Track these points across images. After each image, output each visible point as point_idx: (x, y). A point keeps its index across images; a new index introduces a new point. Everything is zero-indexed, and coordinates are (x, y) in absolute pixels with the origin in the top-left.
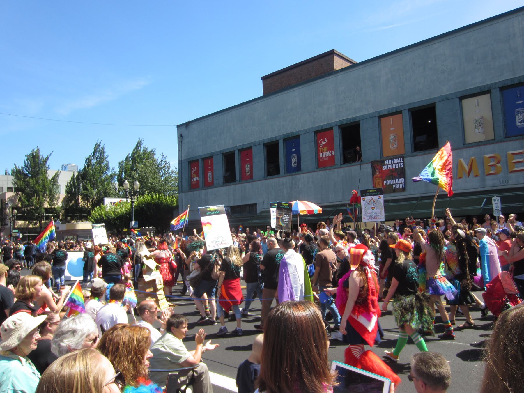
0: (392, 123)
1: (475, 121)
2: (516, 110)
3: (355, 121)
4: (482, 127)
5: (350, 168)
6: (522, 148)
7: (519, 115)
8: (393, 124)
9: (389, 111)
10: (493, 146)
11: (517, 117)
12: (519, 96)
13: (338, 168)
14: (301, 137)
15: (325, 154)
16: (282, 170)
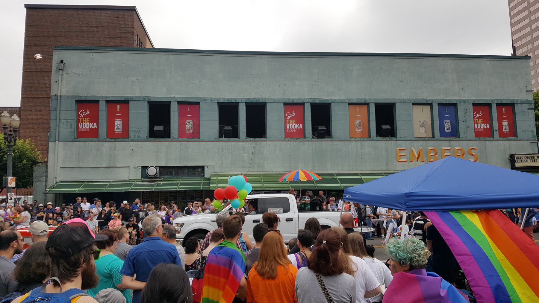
0: (358, 111)
1: (420, 122)
2: (445, 120)
3: (327, 102)
4: (424, 128)
5: (320, 142)
6: (450, 146)
7: (447, 124)
8: (359, 112)
9: (358, 101)
10: (433, 142)
11: (445, 125)
12: (447, 111)
13: (309, 141)
14: (268, 105)
15: (294, 126)
16: (243, 134)
